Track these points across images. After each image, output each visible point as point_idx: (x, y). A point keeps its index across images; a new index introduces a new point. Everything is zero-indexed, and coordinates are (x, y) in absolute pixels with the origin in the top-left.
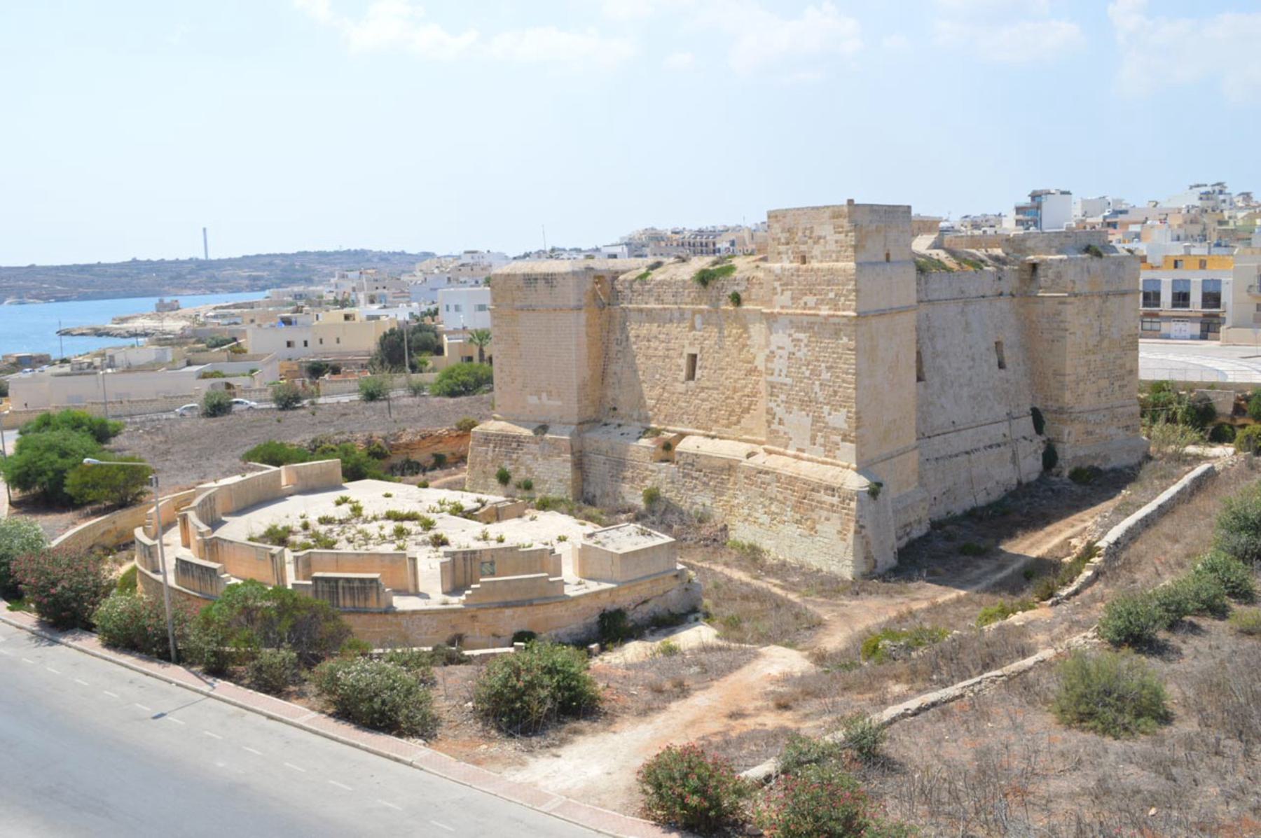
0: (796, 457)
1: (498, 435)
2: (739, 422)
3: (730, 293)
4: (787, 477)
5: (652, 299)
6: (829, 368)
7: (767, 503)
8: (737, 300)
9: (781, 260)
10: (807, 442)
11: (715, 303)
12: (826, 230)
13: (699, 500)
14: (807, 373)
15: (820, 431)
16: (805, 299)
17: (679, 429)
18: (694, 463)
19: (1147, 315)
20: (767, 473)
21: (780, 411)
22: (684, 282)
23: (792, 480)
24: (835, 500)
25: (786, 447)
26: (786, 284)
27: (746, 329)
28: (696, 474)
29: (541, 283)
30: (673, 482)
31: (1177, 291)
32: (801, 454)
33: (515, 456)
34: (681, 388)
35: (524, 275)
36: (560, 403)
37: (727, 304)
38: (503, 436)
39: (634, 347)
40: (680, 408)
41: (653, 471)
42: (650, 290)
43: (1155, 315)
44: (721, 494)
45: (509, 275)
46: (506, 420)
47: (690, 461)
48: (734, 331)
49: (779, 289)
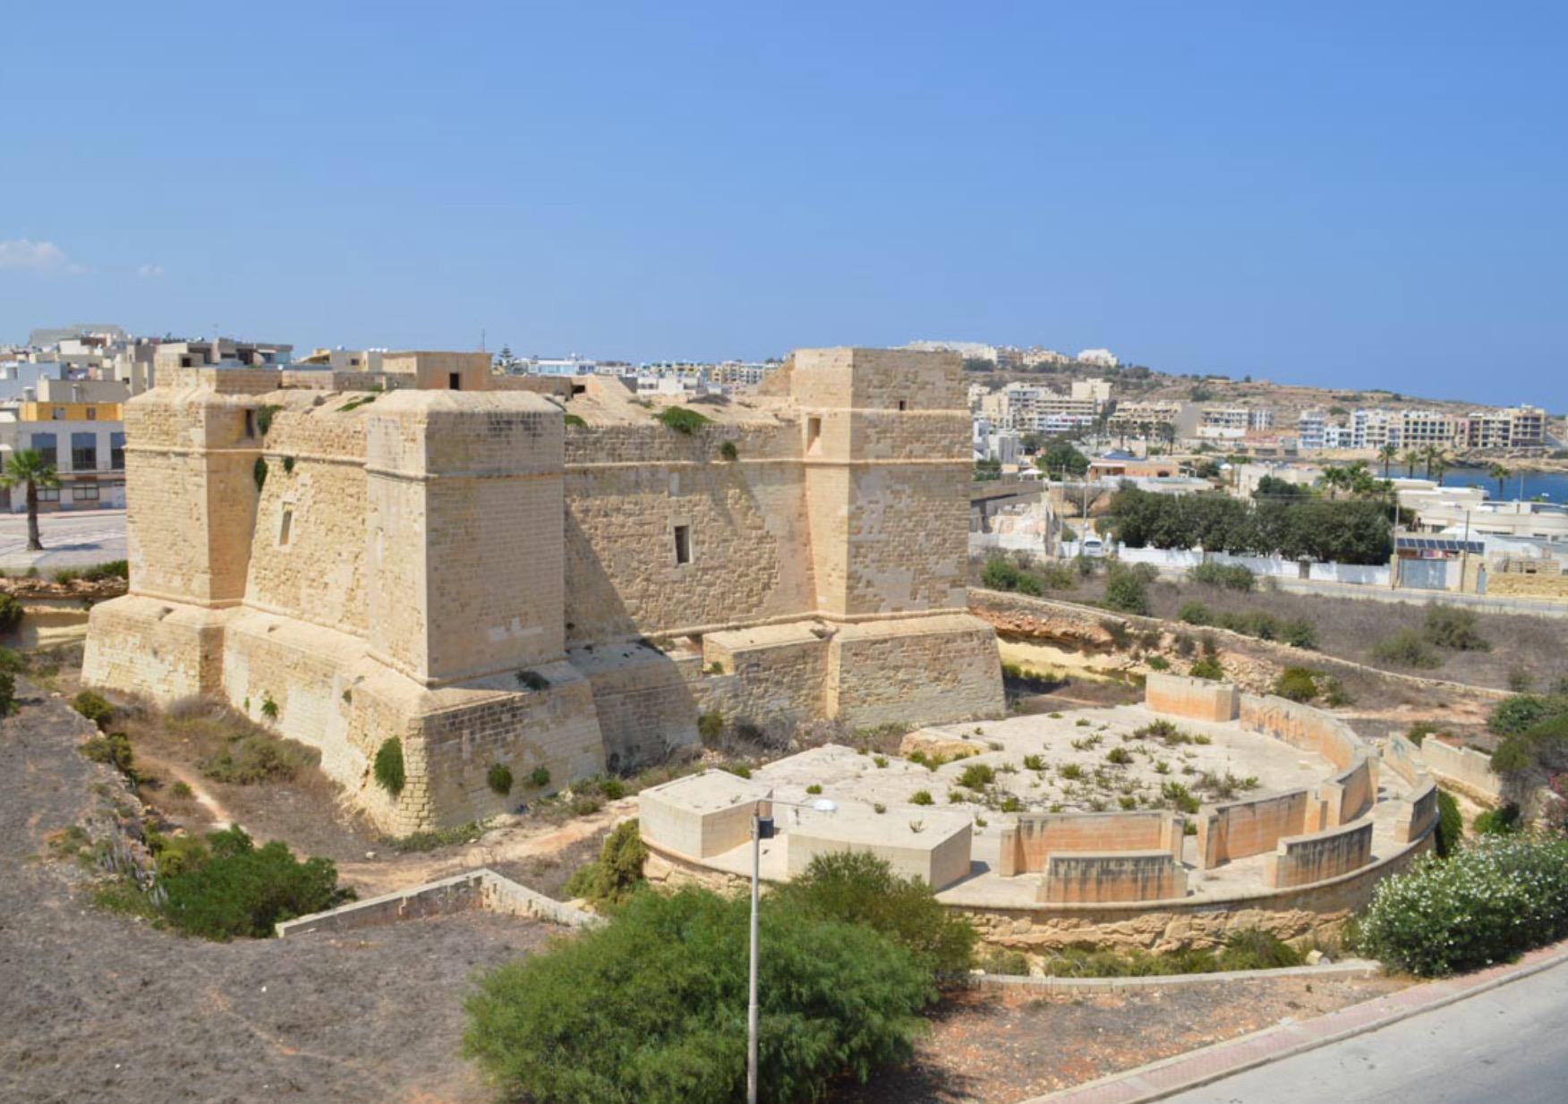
0: (893, 618)
1: (474, 710)
2: (761, 602)
3: (720, 443)
4: (912, 638)
5: (602, 454)
6: (937, 518)
7: (892, 673)
8: (729, 451)
9: (871, 405)
10: (907, 599)
11: (701, 454)
12: (938, 377)
13: (774, 705)
14: (910, 525)
15: (924, 582)
16: (908, 447)
17: (687, 630)
18: (752, 663)
19: (80, 480)
20: (885, 641)
21: (868, 573)
22: (652, 428)
23: (918, 640)
24: (975, 642)
25: (876, 611)
26: (884, 432)
27: (745, 488)
28: (763, 675)
29: (518, 430)
30: (736, 696)
31: (79, 447)
32: (897, 614)
33: (511, 737)
34: (673, 573)
35: (489, 415)
36: (539, 630)
37: (716, 458)
38: (483, 708)
39: (584, 527)
40: (680, 602)
41: (704, 690)
42: (597, 441)
43: (92, 479)
44: (799, 688)
45: (462, 414)
46: (454, 683)
47: (754, 661)
48: (731, 492)
49: (874, 437)
